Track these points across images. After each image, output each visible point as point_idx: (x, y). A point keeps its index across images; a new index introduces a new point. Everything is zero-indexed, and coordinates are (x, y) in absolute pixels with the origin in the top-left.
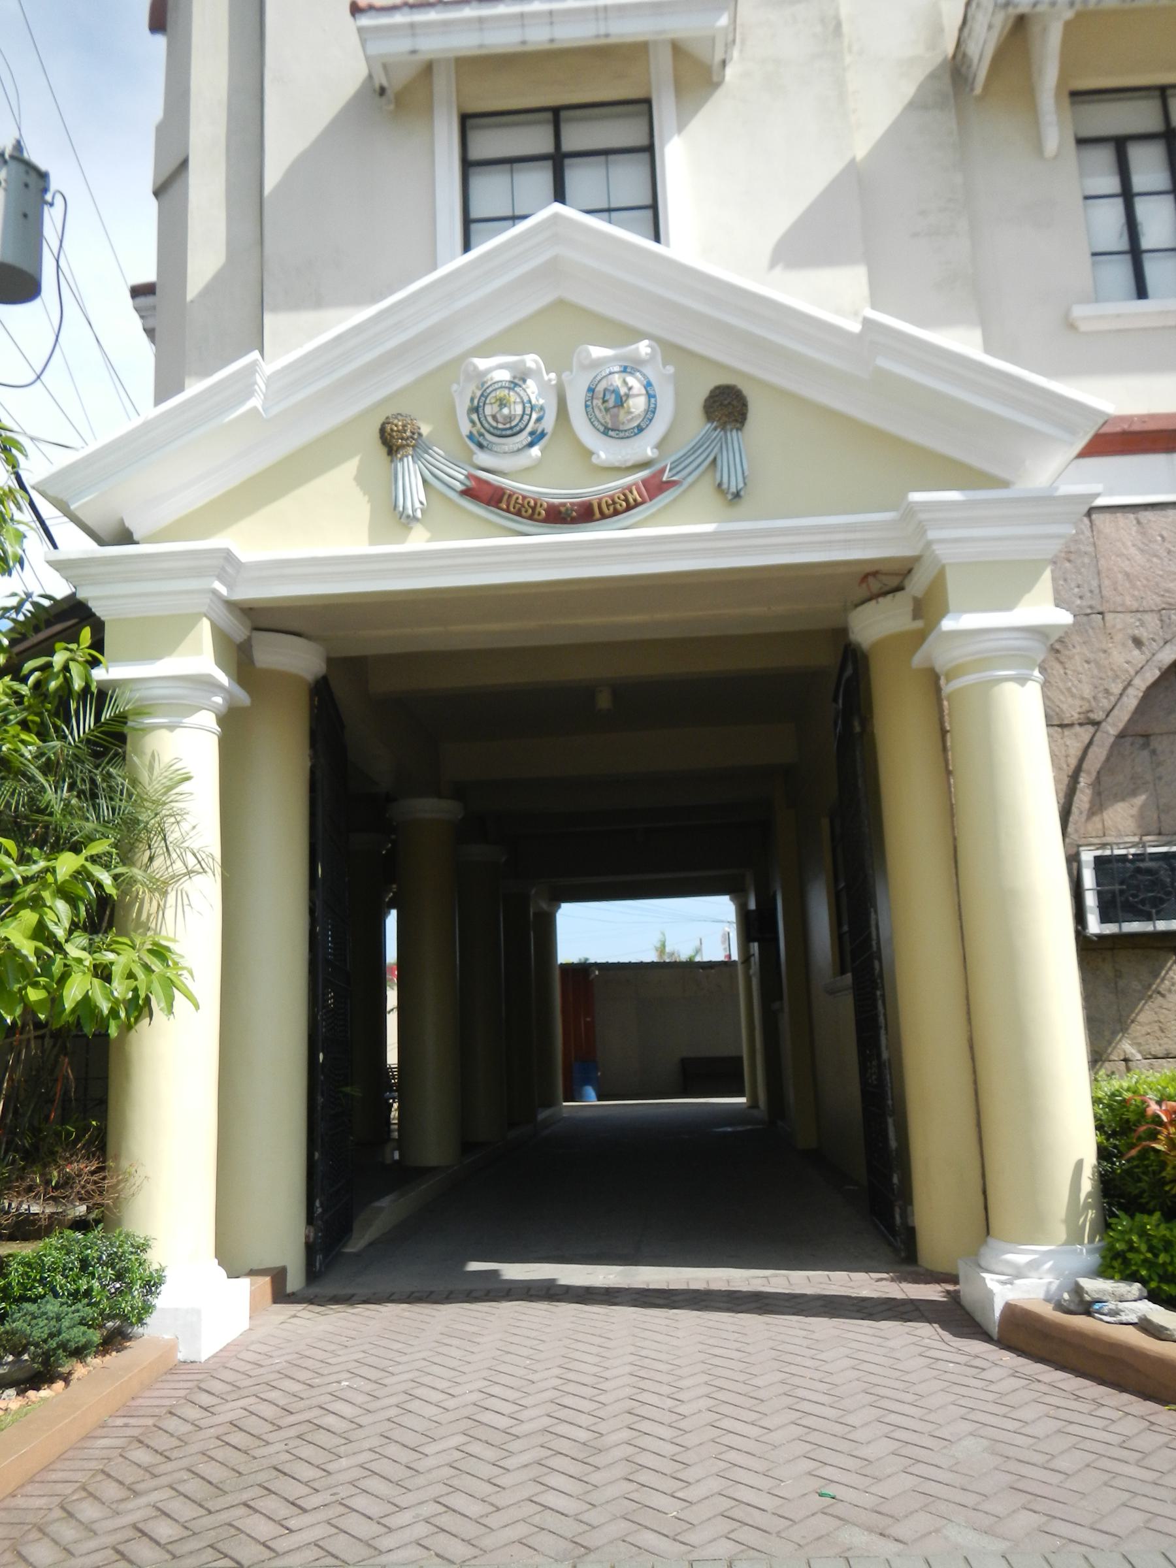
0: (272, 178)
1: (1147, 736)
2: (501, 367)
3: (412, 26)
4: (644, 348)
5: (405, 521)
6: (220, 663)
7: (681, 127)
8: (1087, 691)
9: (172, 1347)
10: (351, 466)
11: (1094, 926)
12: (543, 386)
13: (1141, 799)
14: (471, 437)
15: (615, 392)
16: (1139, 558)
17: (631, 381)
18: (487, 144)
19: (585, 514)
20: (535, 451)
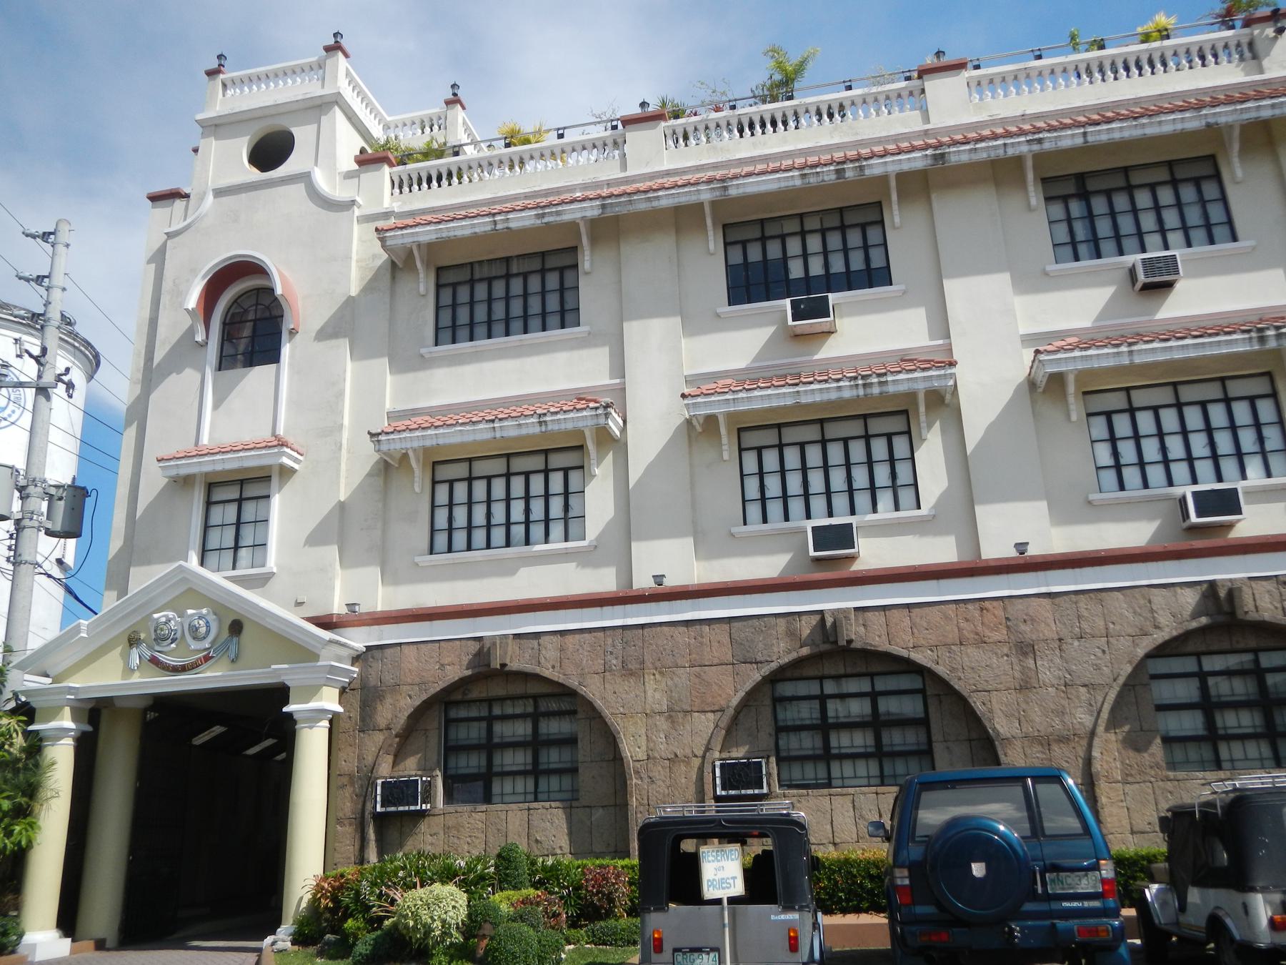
0: (138, 514)
1: (426, 730)
2: (163, 616)
3: (177, 465)
4: (204, 611)
5: (133, 671)
6: (74, 719)
7: (280, 489)
8: (389, 716)
9: (27, 956)
10: (119, 649)
11: (379, 809)
12: (176, 622)
13: (420, 755)
14: (155, 639)
15: (195, 626)
16: (416, 664)
17: (201, 622)
18: (219, 495)
19: (183, 669)
20: (173, 645)
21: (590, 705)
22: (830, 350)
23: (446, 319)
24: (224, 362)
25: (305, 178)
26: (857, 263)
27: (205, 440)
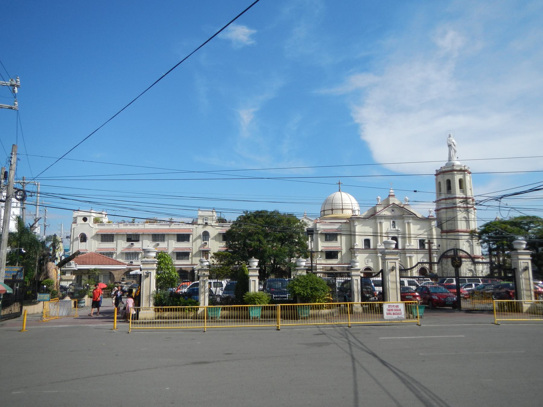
21: (112, 273)
22: (133, 247)
23: (102, 239)
24: (81, 242)
25: (89, 224)
26: (137, 239)
27: (79, 249)
